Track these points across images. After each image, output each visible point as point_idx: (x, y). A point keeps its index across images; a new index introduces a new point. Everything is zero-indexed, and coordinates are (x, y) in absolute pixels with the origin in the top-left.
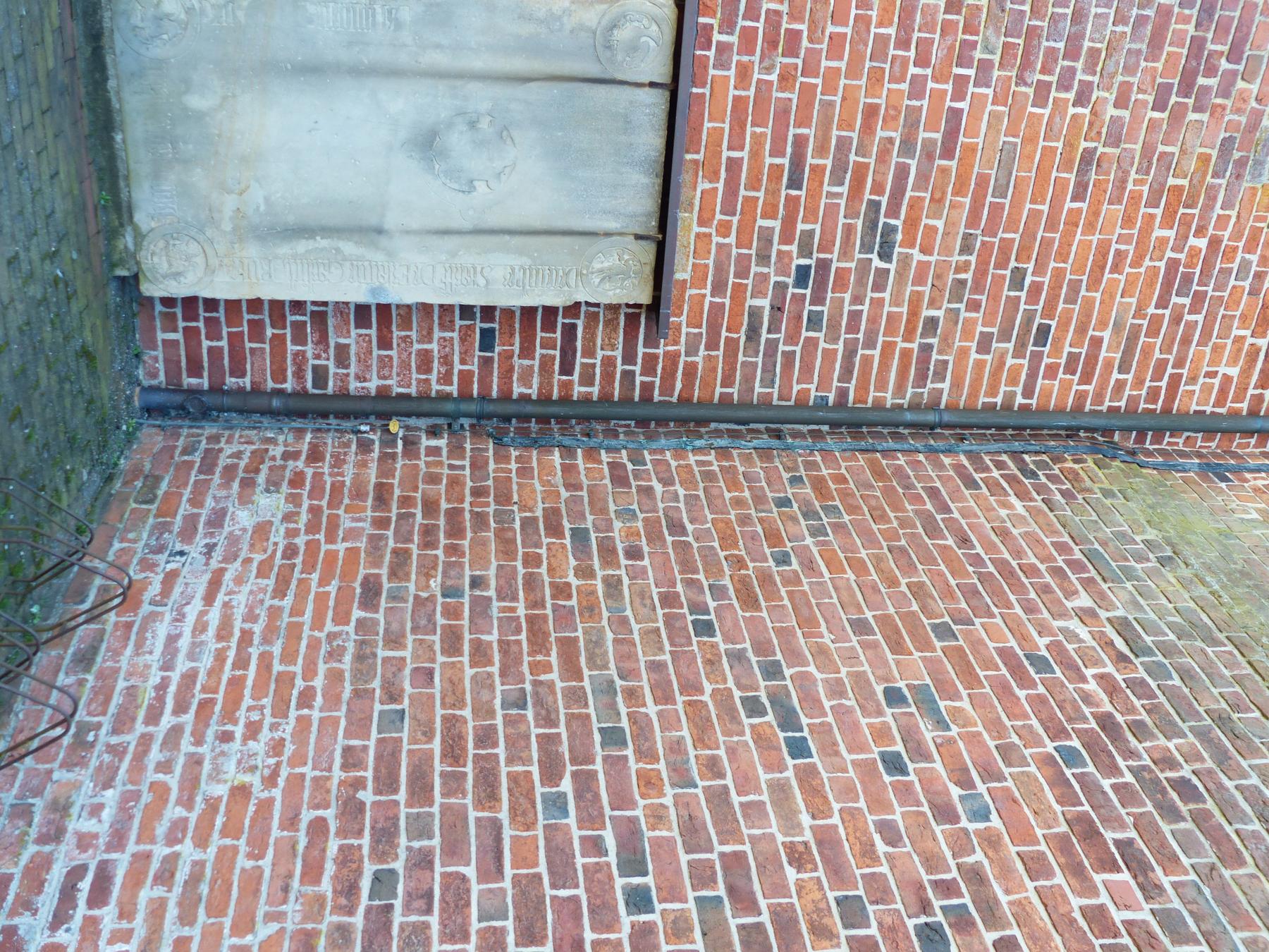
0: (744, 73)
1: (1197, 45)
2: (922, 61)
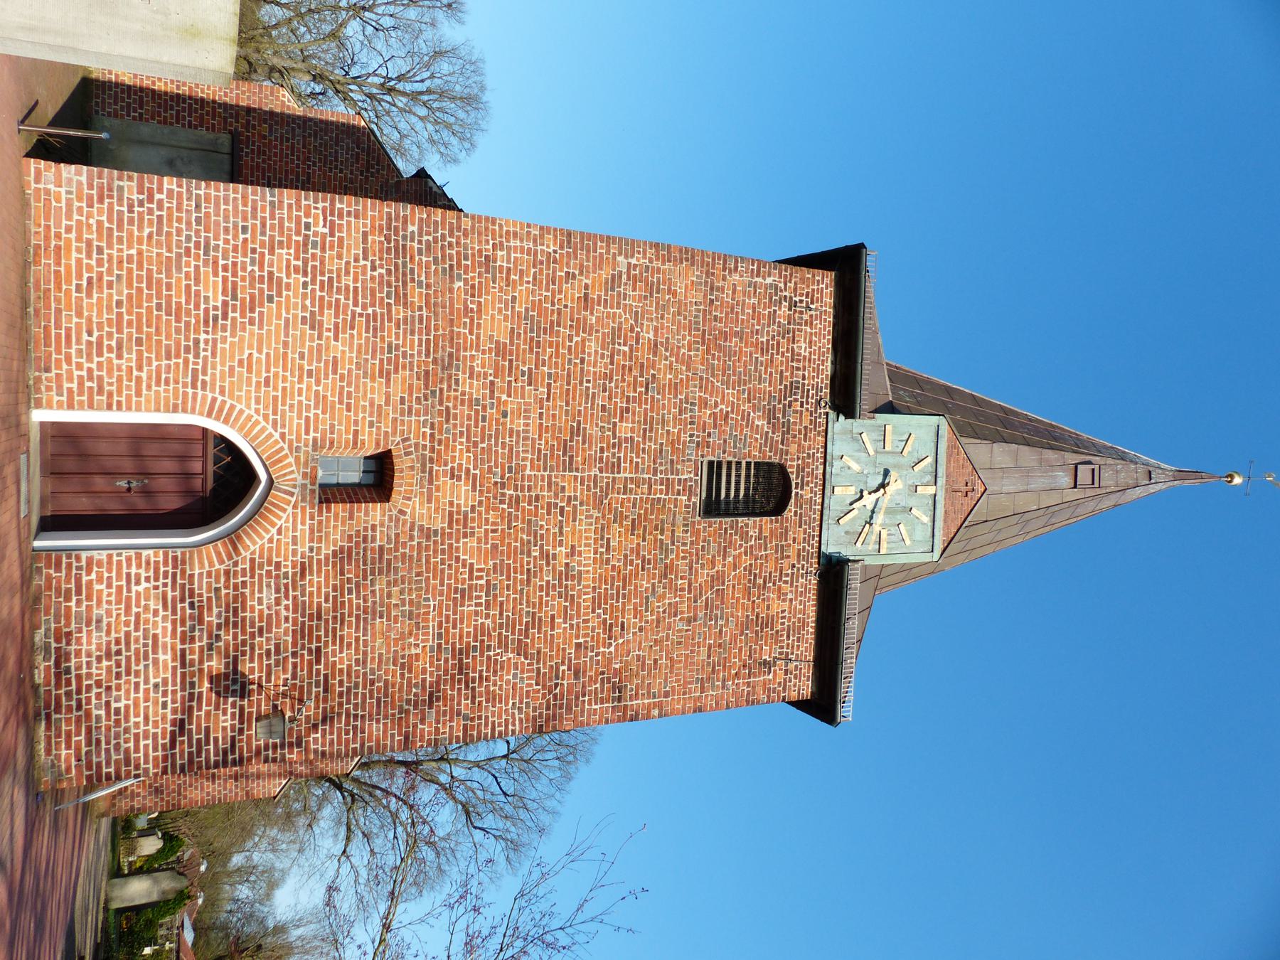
0: (253, 159)
1: (368, 161)
2: (298, 159)
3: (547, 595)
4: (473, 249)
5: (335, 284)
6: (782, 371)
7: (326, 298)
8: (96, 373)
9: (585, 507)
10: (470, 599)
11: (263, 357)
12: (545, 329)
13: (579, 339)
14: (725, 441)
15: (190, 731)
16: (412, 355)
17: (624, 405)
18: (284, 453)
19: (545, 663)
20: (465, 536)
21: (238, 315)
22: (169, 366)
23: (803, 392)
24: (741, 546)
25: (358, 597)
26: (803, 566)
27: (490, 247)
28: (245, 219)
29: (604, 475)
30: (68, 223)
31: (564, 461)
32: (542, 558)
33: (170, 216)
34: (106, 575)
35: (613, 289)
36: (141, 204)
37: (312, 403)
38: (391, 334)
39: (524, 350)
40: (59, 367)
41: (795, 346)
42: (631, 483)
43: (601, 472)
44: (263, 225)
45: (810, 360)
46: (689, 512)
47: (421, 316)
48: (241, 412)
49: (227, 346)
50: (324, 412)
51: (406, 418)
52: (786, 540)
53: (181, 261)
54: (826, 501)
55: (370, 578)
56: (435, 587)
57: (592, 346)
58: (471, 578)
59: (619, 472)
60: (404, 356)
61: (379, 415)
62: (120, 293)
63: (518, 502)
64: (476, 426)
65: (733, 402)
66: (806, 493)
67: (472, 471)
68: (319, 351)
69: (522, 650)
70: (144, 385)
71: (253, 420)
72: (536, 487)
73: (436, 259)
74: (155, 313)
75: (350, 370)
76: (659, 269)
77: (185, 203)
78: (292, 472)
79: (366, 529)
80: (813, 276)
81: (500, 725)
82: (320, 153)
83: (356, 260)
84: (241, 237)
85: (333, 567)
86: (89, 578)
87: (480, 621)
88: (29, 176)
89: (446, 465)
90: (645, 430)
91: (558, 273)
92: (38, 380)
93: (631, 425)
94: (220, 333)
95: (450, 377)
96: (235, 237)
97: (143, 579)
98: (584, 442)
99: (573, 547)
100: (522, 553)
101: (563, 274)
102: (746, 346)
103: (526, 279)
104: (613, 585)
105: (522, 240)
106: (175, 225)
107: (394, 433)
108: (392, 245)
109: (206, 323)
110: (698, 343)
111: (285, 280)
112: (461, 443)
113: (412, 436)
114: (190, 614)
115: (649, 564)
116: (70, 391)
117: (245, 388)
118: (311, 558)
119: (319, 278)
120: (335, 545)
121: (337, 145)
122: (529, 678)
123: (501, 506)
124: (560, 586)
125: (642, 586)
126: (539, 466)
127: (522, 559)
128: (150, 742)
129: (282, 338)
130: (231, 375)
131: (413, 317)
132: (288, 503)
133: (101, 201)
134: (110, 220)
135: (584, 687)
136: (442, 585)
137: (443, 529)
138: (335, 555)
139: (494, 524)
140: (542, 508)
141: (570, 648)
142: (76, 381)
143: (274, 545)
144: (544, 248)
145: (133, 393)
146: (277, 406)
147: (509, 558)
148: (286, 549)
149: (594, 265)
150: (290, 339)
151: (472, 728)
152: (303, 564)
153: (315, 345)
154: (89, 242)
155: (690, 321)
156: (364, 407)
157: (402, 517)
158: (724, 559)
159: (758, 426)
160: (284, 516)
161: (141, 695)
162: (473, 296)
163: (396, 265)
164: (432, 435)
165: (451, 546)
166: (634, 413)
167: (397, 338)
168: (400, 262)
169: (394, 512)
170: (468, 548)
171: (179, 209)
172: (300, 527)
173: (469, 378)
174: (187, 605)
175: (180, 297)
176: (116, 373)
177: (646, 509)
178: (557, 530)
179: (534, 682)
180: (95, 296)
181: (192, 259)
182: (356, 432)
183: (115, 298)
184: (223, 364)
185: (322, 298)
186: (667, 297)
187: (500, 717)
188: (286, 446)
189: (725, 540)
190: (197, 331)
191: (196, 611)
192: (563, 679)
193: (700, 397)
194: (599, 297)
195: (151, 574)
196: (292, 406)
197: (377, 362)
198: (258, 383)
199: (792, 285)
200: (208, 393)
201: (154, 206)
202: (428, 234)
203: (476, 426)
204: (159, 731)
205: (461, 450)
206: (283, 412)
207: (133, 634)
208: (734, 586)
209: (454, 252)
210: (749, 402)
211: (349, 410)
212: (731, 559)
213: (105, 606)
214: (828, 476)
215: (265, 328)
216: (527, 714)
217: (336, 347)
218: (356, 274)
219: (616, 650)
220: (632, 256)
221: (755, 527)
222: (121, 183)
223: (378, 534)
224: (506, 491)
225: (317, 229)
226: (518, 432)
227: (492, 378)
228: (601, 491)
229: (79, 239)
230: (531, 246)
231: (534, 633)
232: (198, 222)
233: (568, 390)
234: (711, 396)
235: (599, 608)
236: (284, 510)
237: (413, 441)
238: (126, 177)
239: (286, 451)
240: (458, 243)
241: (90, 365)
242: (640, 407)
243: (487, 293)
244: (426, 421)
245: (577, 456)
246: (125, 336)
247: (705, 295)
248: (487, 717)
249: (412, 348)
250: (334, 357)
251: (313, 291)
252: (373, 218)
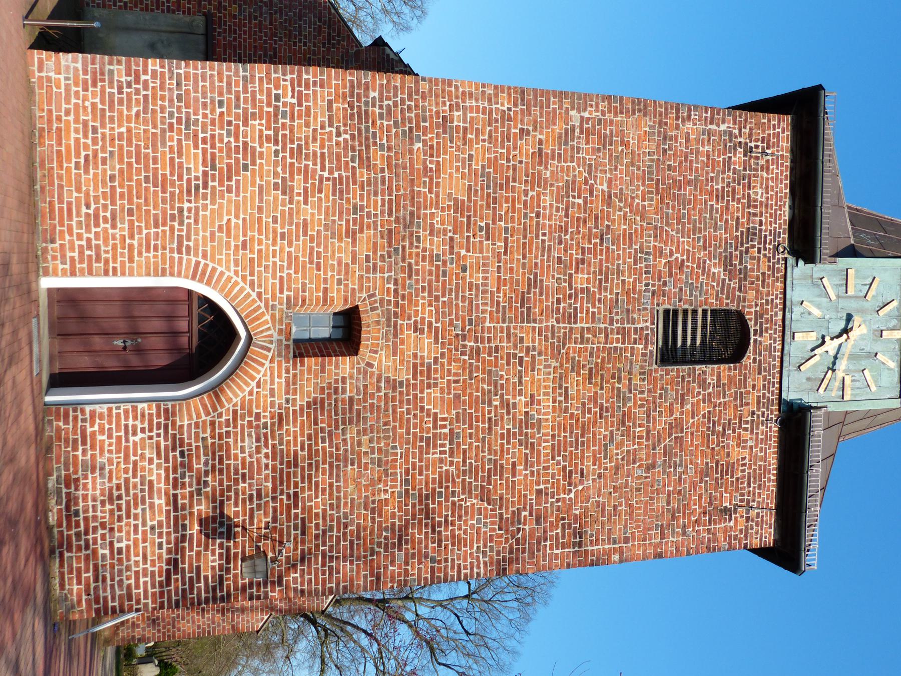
0: (225, 38)
1: (329, 34)
2: (266, 36)
3: (508, 443)
4: (430, 110)
5: (304, 151)
6: (738, 218)
7: (296, 165)
8: (94, 242)
9: (543, 357)
10: (435, 447)
11: (240, 222)
12: (501, 185)
13: (534, 193)
14: (681, 289)
15: (183, 569)
16: (376, 215)
17: (580, 257)
18: (260, 311)
19: (507, 509)
20: (429, 387)
21: (216, 184)
22: (157, 234)
23: (760, 238)
24: (699, 393)
25: (331, 446)
26: (763, 413)
27: (447, 108)
28: (221, 94)
29: (562, 325)
30: (68, 106)
31: (522, 312)
32: (502, 407)
33: (154, 95)
34: (107, 426)
35: (566, 144)
36: (129, 85)
37: (285, 264)
38: (356, 196)
39: (482, 206)
40: (62, 238)
41: (751, 192)
42: (588, 333)
43: (558, 322)
44: (238, 98)
45: (767, 206)
46: (645, 361)
47: (383, 178)
48: (222, 273)
49: (208, 213)
50: (296, 272)
51: (371, 275)
52: (745, 387)
53: (165, 136)
54: (786, 348)
55: (341, 427)
56: (401, 437)
57: (547, 200)
58: (435, 427)
59: (575, 323)
60: (369, 217)
61: (347, 273)
62: (113, 168)
63: (478, 353)
64: (437, 281)
65: (688, 250)
66: (765, 340)
67: (434, 324)
68: (291, 215)
69: (485, 496)
70: (136, 251)
71: (233, 281)
72: (495, 338)
73: (396, 122)
74: (144, 185)
75: (319, 232)
76: (611, 122)
77: (168, 82)
78: (269, 329)
79: (336, 381)
80: (769, 121)
81: (465, 568)
82: (285, 29)
83: (322, 127)
84: (218, 111)
85: (307, 417)
86: (92, 429)
87: (445, 468)
88: (34, 66)
89: (409, 319)
90: (600, 281)
91: (513, 130)
92: (45, 250)
93: (586, 276)
94: (201, 202)
95: (411, 235)
96: (213, 111)
97: (139, 430)
98: (541, 294)
99: (532, 396)
100: (483, 403)
101: (518, 131)
102: (701, 194)
103: (481, 137)
104: (571, 433)
105: (477, 100)
106: (159, 102)
107: (361, 290)
108: (355, 111)
109: (189, 192)
110: (652, 192)
111: (258, 149)
112: (423, 298)
113: (377, 292)
114: (181, 462)
115: (607, 411)
116: (72, 259)
117: (224, 251)
118: (287, 409)
119: (289, 146)
120: (309, 397)
121: (300, 20)
122: (492, 523)
123: (463, 357)
124: (521, 435)
125: (600, 433)
126: (498, 318)
127: (483, 408)
128: (148, 579)
129: (257, 204)
130: (212, 240)
131: (376, 179)
132: (266, 357)
133: (94, 85)
134: (103, 102)
135: (545, 532)
136: (408, 433)
137: (407, 380)
138: (309, 406)
139: (456, 374)
140: (502, 358)
141: (531, 494)
142: (77, 250)
143: (254, 397)
144: (499, 106)
145: (126, 259)
146: (254, 267)
147: (470, 408)
148: (265, 401)
149: (548, 120)
150: (264, 205)
151: (440, 569)
152: (280, 415)
153: (287, 209)
154: (85, 123)
155: (644, 171)
156: (333, 265)
157: (370, 370)
158: (682, 407)
159: (714, 273)
160: (262, 370)
161: (140, 536)
162: (432, 156)
163: (359, 130)
164: (396, 291)
165: (415, 396)
166: (589, 265)
167: (362, 200)
168: (363, 127)
169: (363, 365)
170: (432, 398)
171: (162, 88)
172: (276, 380)
173: (430, 235)
174: (178, 453)
175: (165, 169)
176: (111, 242)
177: (603, 358)
178: (516, 380)
179: (497, 527)
180: (92, 171)
181: (174, 134)
182: (326, 290)
183: (109, 173)
184: (205, 230)
185: (292, 165)
186: (620, 148)
187: (465, 560)
188: (262, 305)
189: (683, 387)
190: (181, 200)
191: (186, 459)
192: (525, 525)
193: (655, 246)
194: (553, 151)
195: (146, 425)
196: (267, 267)
197: (344, 223)
198: (236, 247)
199: (747, 131)
200: (192, 257)
201: (141, 86)
202: (388, 99)
203: (437, 281)
204: (156, 569)
205: (423, 304)
206: (260, 272)
207: (132, 480)
208: (692, 434)
209: (413, 115)
210: (705, 249)
211: (319, 269)
212: (689, 407)
213: (107, 455)
214: (787, 322)
215: (242, 195)
216: (491, 558)
217: (306, 210)
218: (322, 140)
219: (576, 496)
220: (585, 110)
221: (712, 375)
222: (112, 67)
223: (348, 385)
224: (466, 342)
225: (286, 100)
226: (477, 286)
227: (451, 234)
228: (559, 341)
229: (76, 121)
230: (486, 105)
231: (496, 481)
232: (180, 100)
233: (524, 243)
234: (666, 245)
235: (559, 455)
236: (262, 365)
237: (378, 297)
238: (115, 62)
239: (263, 309)
240: (417, 106)
241: (88, 235)
242: (595, 258)
243: (445, 153)
244: (389, 277)
245: (535, 308)
246: (118, 207)
247: (658, 145)
248: (453, 560)
249: (376, 209)
250: (304, 220)
251: (284, 158)
252: (337, 86)
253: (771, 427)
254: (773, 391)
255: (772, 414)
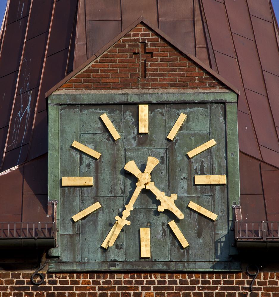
54: (160, 267)
214: (128, 267)
253: (260, 283)
254: (215, 282)
255: (242, 283)
